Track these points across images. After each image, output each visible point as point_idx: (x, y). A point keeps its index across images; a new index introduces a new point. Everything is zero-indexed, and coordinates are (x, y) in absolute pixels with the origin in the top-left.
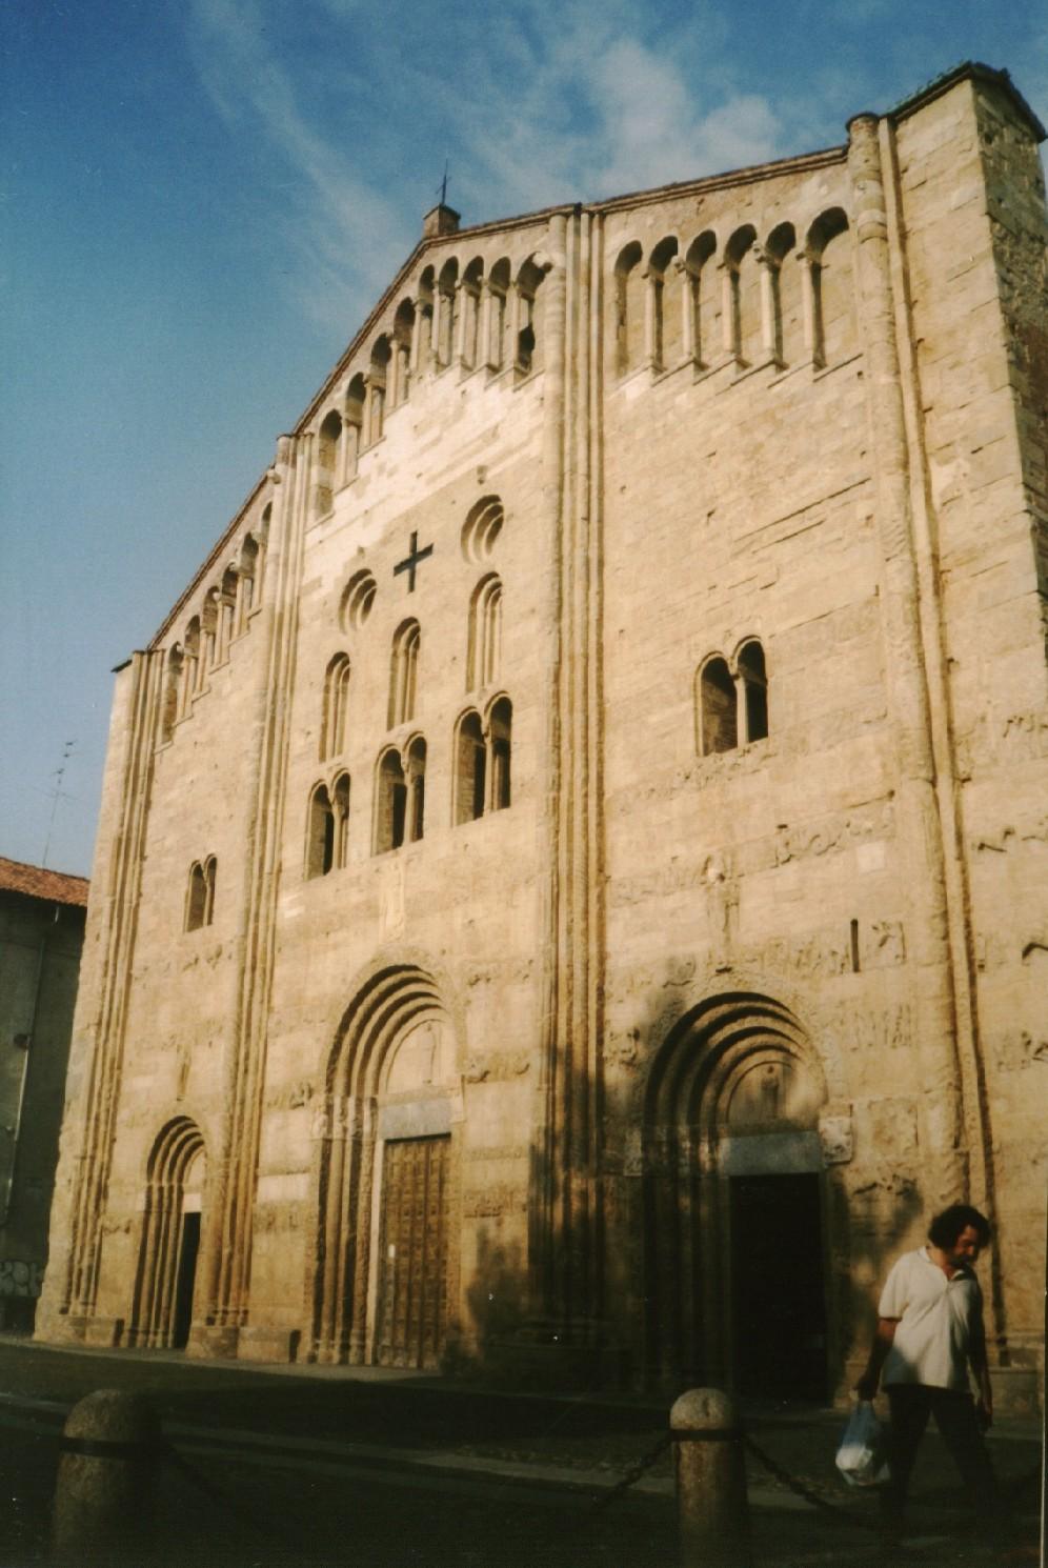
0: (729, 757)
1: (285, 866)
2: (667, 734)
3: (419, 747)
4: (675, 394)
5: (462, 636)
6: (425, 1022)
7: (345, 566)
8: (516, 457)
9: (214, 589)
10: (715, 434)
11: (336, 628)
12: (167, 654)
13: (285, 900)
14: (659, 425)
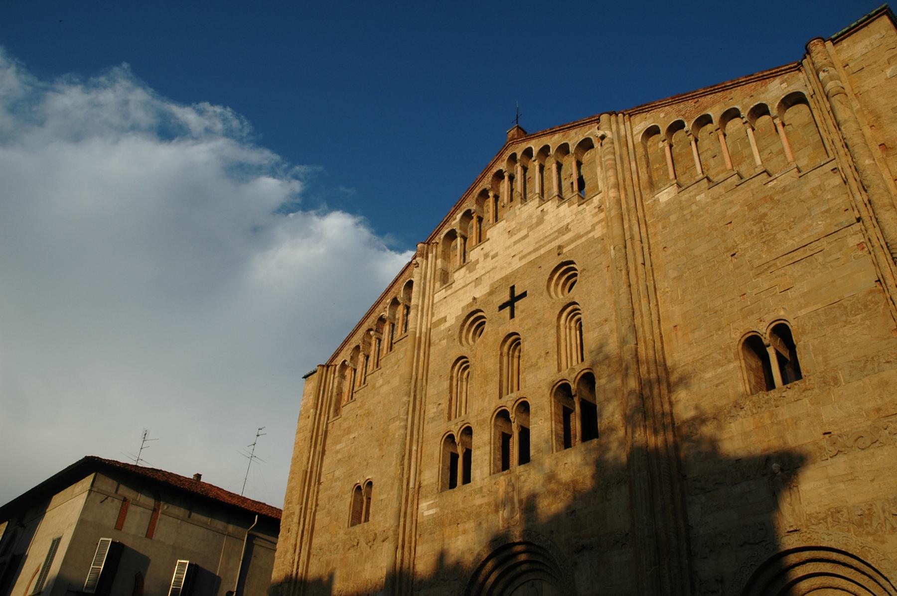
0: (772, 394)
1: (424, 483)
2: (722, 383)
3: (524, 407)
4: (696, 195)
5: (552, 340)
6: (528, 581)
7: (463, 309)
8: (584, 239)
9: (370, 330)
10: (729, 212)
11: (457, 343)
12: (338, 367)
13: (424, 505)
14: (685, 212)
